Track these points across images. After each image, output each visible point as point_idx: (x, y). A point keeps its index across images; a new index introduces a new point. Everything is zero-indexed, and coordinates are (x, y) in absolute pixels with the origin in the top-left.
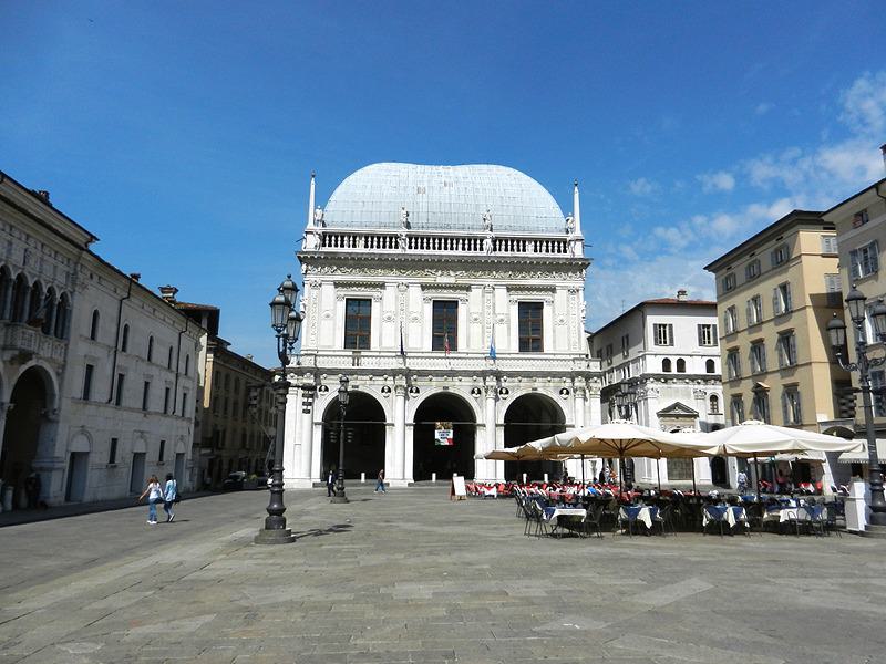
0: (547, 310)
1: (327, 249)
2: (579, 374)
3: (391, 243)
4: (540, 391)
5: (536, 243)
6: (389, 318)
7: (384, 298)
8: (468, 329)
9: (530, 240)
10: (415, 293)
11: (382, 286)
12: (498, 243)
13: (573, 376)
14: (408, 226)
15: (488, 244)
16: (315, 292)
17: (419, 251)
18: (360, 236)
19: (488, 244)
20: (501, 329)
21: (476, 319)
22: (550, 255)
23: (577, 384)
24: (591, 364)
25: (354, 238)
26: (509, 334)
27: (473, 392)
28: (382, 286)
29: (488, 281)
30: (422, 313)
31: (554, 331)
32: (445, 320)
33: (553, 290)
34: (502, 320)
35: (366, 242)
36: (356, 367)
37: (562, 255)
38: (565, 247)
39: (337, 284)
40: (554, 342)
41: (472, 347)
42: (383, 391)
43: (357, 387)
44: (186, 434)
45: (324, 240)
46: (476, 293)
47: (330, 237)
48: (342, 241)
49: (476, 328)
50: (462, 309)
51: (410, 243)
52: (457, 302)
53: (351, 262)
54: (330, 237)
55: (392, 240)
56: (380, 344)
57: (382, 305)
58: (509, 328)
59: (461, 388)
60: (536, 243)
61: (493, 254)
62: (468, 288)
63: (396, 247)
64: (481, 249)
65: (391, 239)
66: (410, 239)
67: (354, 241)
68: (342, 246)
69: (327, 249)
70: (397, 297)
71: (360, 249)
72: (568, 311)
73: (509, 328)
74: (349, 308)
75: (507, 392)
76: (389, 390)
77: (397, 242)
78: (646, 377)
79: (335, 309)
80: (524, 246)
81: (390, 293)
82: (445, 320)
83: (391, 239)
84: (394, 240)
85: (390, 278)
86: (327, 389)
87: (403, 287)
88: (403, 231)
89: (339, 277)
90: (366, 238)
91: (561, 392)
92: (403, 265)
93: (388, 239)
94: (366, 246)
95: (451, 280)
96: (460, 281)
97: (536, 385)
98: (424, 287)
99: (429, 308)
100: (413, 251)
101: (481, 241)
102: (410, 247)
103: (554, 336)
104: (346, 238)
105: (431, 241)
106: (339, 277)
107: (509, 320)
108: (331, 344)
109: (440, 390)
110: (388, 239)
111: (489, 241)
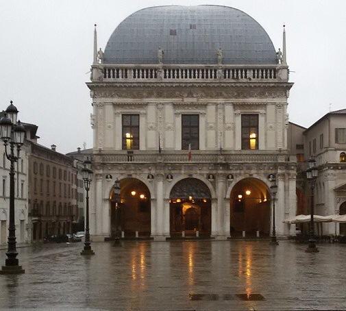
0: (261, 119)
1: (107, 80)
2: (281, 164)
3: (151, 74)
4: (255, 176)
5: (254, 71)
6: (151, 127)
7: (148, 113)
8: (206, 134)
9: (250, 69)
10: (169, 110)
11: (147, 104)
12: (227, 72)
13: (276, 166)
14: (163, 61)
15: (220, 72)
16: (100, 111)
17: (171, 80)
18: (130, 69)
19: (220, 72)
20: (229, 134)
21: (211, 127)
22: (265, 80)
23: (279, 171)
24: (291, 157)
25: (126, 70)
26: (234, 137)
27: (209, 178)
28: (147, 104)
29: (221, 100)
30: (174, 123)
31: (266, 134)
32: (190, 129)
33: (264, 105)
34: (229, 128)
35: (135, 74)
36: (130, 162)
37: (272, 80)
38: (275, 74)
39: (115, 105)
40: (266, 142)
41: (208, 146)
42: (148, 177)
43: (131, 175)
44: (24, 207)
45: (105, 73)
46: (211, 109)
47: (109, 71)
48: (118, 73)
49: (212, 133)
50: (202, 121)
51: (165, 73)
52: (198, 115)
53: (124, 89)
54: (109, 71)
55: (152, 72)
56: (146, 146)
57: (146, 118)
58: (234, 133)
59: (200, 175)
60: (254, 71)
61: (225, 80)
62: (205, 105)
63: (156, 77)
64: (215, 77)
65: (151, 71)
66: (165, 71)
67: (126, 74)
68: (118, 77)
69: (107, 80)
70: (157, 113)
71: (130, 79)
72: (276, 122)
73: (234, 133)
74: (125, 120)
75: (232, 178)
76: (153, 177)
77: (156, 74)
78: (329, 166)
79: (114, 123)
80: (246, 74)
81: (151, 110)
82: (190, 129)
83: (151, 71)
84: (154, 72)
85: (153, 100)
86: (111, 177)
87: (160, 106)
88: (160, 65)
89: (116, 100)
90: (135, 71)
91: (269, 177)
92: (161, 91)
93: (149, 71)
94: (135, 77)
95: (194, 100)
96: (203, 100)
97: (253, 172)
98: (175, 106)
99: (179, 120)
100: (167, 80)
101: (215, 71)
102: (165, 77)
103: (266, 138)
104: (120, 71)
105: (180, 72)
106: (116, 100)
107: (234, 128)
108: (113, 146)
109: (186, 177)
110: (149, 71)
111: (220, 71)
